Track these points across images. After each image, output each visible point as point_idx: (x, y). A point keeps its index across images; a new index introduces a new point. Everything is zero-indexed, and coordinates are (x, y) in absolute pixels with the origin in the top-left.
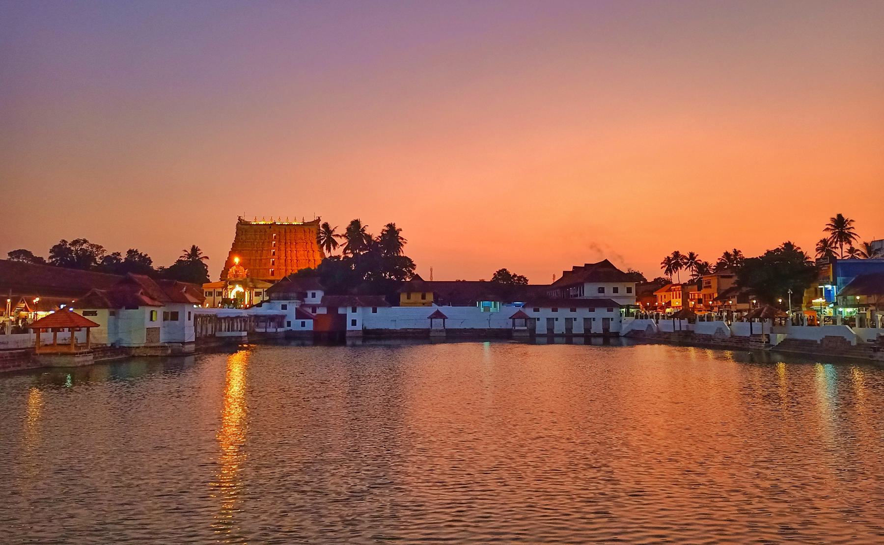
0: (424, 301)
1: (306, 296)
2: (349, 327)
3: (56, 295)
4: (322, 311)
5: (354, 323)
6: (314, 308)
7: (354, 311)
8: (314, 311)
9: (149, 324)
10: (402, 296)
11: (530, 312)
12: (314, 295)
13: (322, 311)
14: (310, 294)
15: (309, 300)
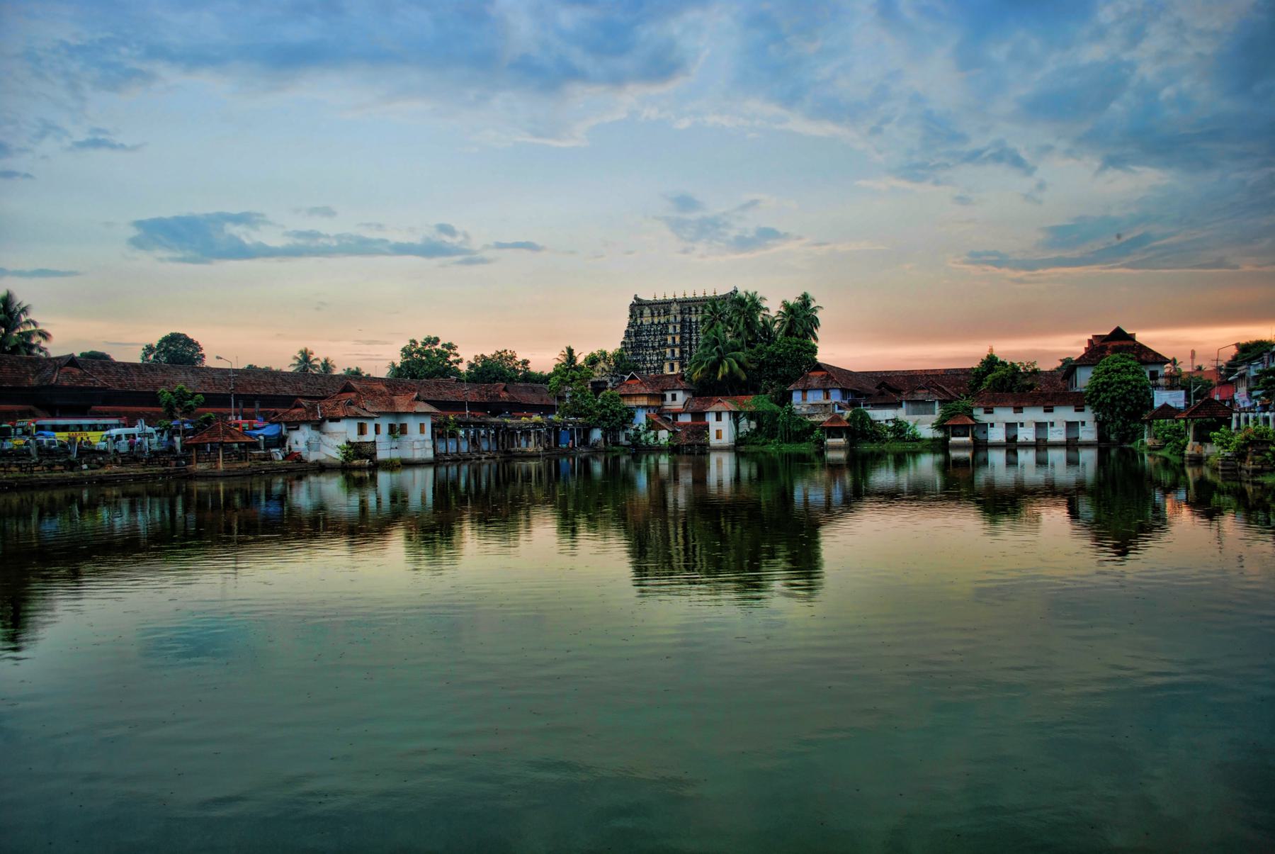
0: (827, 402)
1: (663, 398)
2: (713, 441)
3: (53, 416)
4: (686, 419)
5: (718, 436)
6: (676, 415)
7: (719, 418)
8: (676, 418)
9: (354, 438)
10: (794, 395)
11: (980, 415)
12: (674, 397)
13: (686, 419)
14: (669, 395)
15: (669, 404)
